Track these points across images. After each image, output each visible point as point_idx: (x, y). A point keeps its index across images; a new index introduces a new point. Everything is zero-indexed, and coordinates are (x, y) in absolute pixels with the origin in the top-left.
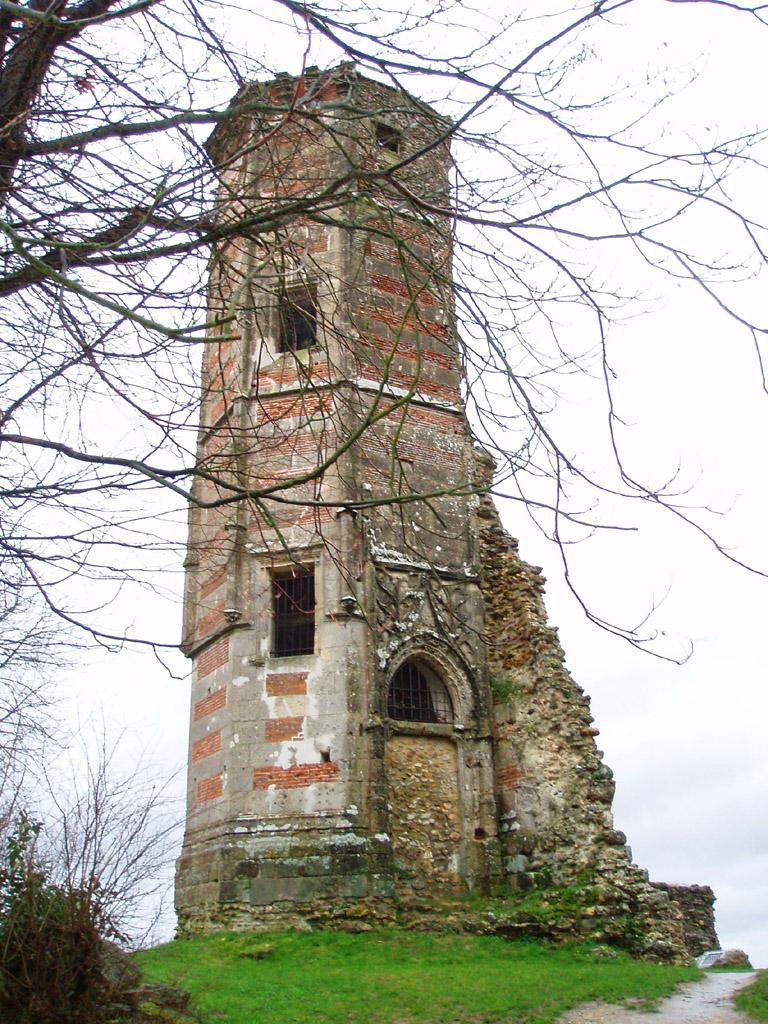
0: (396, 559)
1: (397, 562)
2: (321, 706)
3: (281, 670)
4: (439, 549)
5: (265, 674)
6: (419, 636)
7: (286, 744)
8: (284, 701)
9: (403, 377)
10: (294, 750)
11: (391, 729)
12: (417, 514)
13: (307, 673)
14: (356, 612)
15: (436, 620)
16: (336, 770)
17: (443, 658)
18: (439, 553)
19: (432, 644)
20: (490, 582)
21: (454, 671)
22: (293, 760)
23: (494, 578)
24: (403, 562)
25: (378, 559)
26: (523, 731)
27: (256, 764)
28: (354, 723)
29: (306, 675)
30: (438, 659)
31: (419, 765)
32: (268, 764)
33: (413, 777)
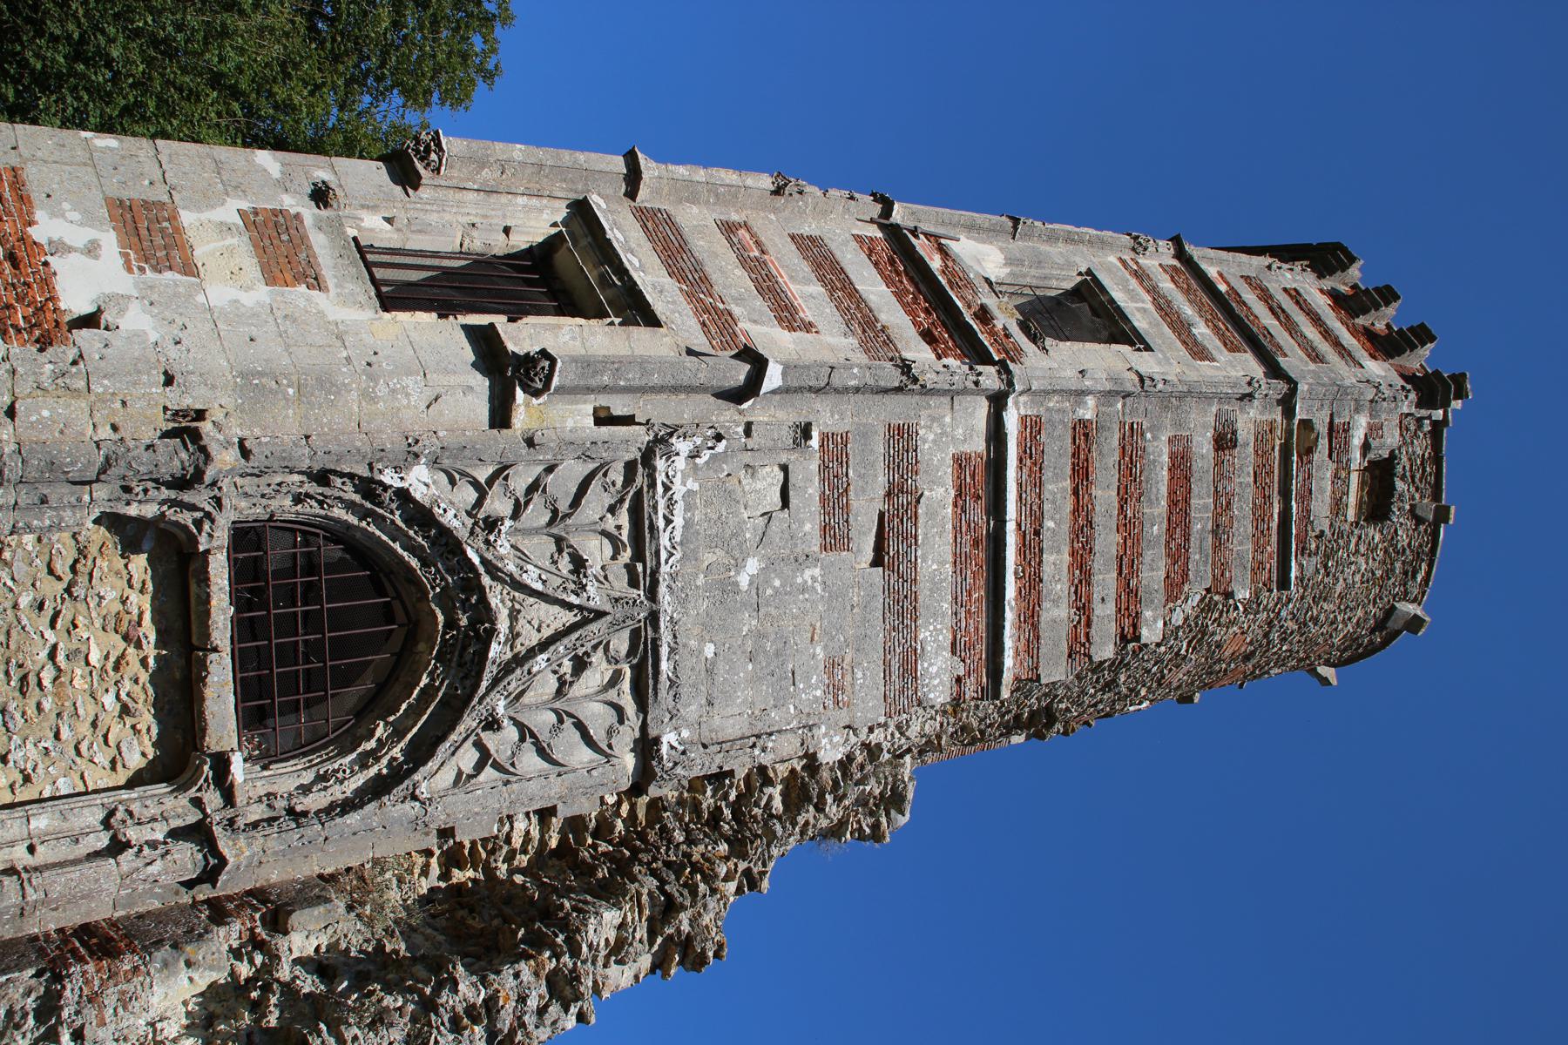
0: (668, 521)
1: (661, 523)
2: (237, 313)
3: (319, 242)
4: (709, 650)
5: (299, 209)
6: (483, 600)
7: (110, 241)
8: (231, 241)
9: (1037, 533)
10: (92, 250)
11: (198, 524)
12: (777, 583)
13: (328, 291)
14: (520, 394)
15: (532, 653)
16: (44, 343)
17: (428, 692)
18: (701, 651)
19: (464, 648)
20: (650, 824)
21: (398, 733)
22: (60, 248)
23: (665, 833)
24: (664, 541)
25: (660, 464)
26: (259, 959)
27: (31, 173)
28: (203, 390)
29: (317, 283)
30: (425, 680)
31: (95, 658)
32: (37, 196)
33: (51, 636)
